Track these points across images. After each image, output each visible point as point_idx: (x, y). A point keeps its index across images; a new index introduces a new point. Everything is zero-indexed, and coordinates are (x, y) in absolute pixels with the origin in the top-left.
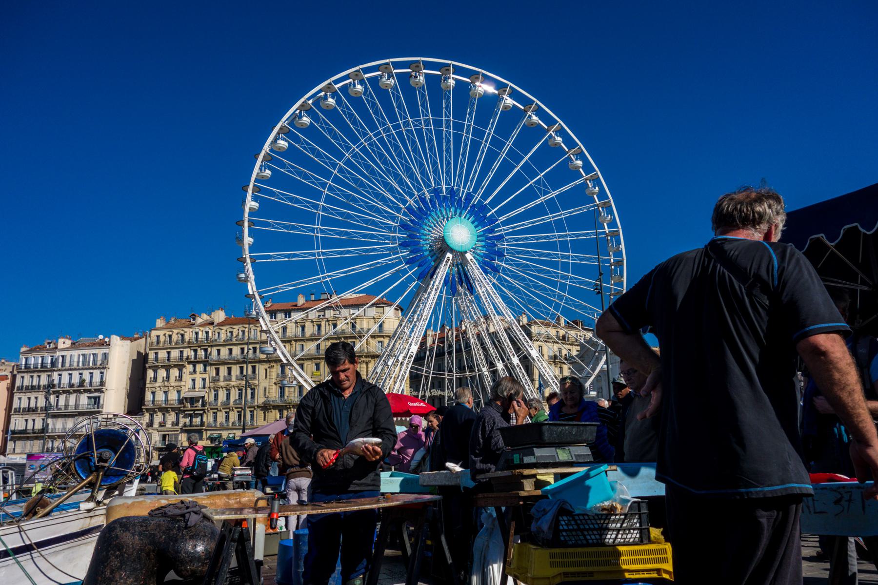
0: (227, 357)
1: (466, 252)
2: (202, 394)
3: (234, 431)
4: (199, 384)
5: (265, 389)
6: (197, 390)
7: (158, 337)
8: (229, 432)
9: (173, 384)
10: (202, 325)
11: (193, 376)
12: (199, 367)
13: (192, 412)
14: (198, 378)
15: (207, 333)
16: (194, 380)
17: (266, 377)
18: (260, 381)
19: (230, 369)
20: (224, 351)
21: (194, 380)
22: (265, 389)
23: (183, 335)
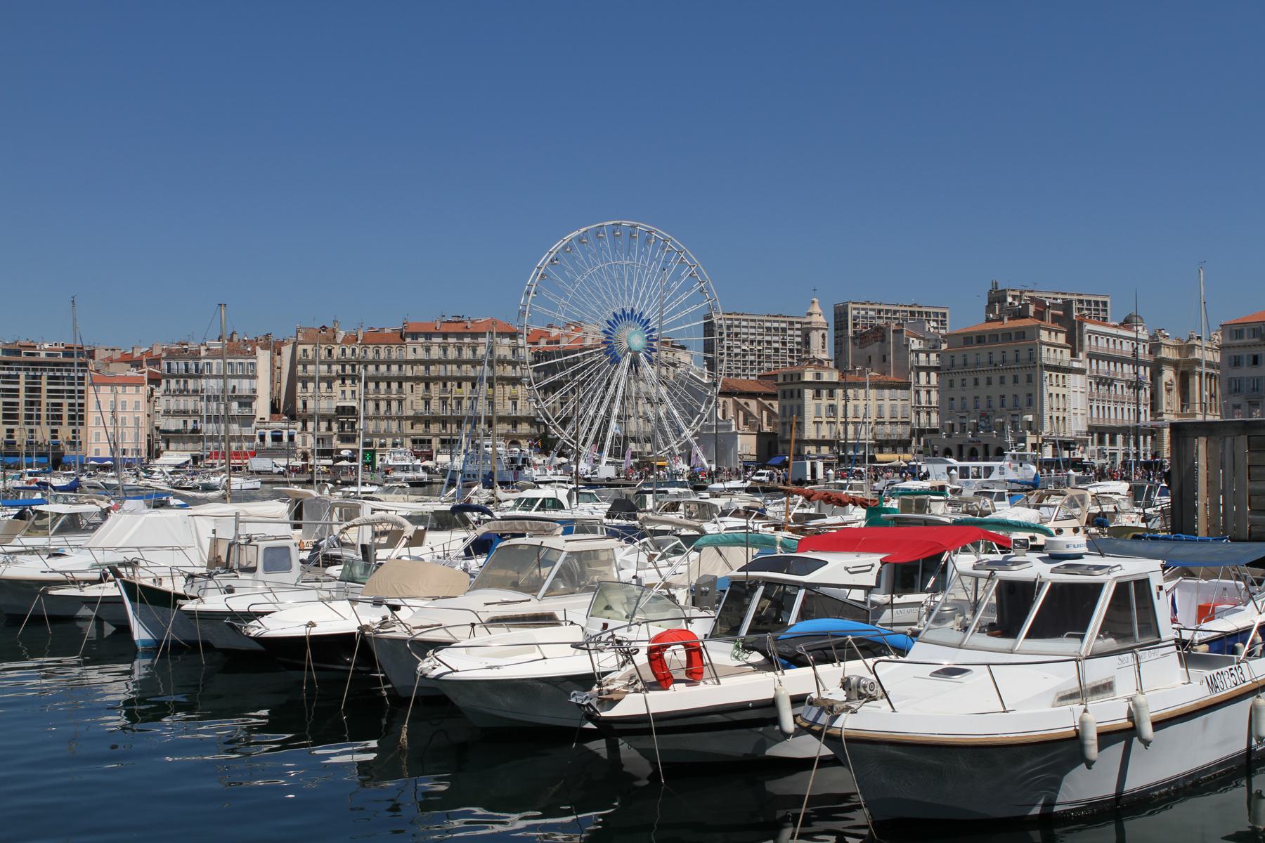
1: (640, 352)
2: (354, 404)
4: (348, 394)
5: (412, 402)
6: (348, 400)
7: (305, 351)
9: (324, 394)
10: (345, 341)
11: (343, 388)
15: (354, 350)
16: (343, 392)
17: (412, 392)
19: (389, 386)
21: (343, 392)
22: (412, 402)
23: (330, 351)
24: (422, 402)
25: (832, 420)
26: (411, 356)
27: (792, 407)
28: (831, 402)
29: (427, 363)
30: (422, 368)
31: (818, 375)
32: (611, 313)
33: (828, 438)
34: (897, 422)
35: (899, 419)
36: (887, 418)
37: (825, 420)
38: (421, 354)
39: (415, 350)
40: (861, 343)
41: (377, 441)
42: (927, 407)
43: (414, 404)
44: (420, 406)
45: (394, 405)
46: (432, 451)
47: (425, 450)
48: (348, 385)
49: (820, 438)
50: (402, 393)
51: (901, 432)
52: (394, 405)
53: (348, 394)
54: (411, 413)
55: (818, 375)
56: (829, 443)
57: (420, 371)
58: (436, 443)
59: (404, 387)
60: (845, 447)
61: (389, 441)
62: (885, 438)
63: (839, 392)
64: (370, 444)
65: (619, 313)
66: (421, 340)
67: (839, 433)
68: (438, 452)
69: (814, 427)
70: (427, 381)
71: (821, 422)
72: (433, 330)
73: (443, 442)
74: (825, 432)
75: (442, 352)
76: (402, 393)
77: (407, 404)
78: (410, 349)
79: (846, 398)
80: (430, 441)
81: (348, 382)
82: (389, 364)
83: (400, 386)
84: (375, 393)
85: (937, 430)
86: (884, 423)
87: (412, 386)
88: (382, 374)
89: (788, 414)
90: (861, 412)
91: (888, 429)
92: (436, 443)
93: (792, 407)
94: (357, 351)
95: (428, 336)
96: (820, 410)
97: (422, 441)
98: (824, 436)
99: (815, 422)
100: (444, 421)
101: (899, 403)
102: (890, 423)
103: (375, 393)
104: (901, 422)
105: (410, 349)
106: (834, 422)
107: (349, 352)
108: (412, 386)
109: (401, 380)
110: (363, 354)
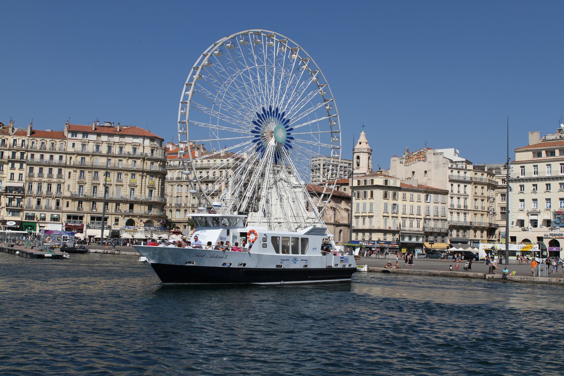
0: (39, 161)
2: (21, 185)
3: (45, 213)
4: (16, 177)
5: (69, 186)
8: (41, 213)
11: (12, 171)
12: (17, 165)
13: (13, 197)
14: (17, 173)
18: (65, 180)
20: (37, 156)
22: (69, 186)
24: (77, 186)
25: (395, 215)
26: (70, 149)
27: (365, 205)
28: (395, 202)
29: (83, 155)
30: (79, 158)
31: (386, 181)
32: (255, 113)
33: (392, 229)
34: (438, 220)
35: (440, 217)
36: (432, 217)
37: (390, 215)
38: (78, 147)
39: (74, 144)
40: (406, 162)
41: (37, 214)
42: (458, 210)
43: (71, 187)
44: (75, 189)
45: (54, 187)
46: (83, 226)
47: (77, 225)
48: (17, 169)
49: (387, 228)
50: (61, 178)
51: (441, 226)
52: (54, 187)
53: (16, 177)
54: (68, 194)
55: (386, 181)
56: (394, 232)
57: (77, 160)
58: (87, 219)
59: (63, 173)
60: (403, 236)
61: (48, 216)
62: (431, 231)
63: (400, 194)
64: (33, 217)
65: (267, 109)
66: (80, 136)
67: (400, 225)
68: (88, 227)
69: (382, 220)
70: (82, 168)
71: (388, 217)
72: (89, 131)
73: (93, 218)
74: (391, 224)
75: (95, 148)
76: (61, 178)
77: (64, 188)
78: (70, 143)
79: (404, 199)
80: (81, 218)
81: (17, 165)
82: (52, 152)
83: (60, 172)
84: (39, 176)
85: (523, 226)
86: (430, 219)
87: (70, 173)
88: (46, 162)
89: (361, 210)
90: (415, 211)
91: (432, 224)
92: (87, 219)
93: (365, 205)
94: (26, 143)
95: (85, 134)
96: (387, 207)
97: (75, 218)
98: (390, 227)
99: (384, 216)
100: (94, 201)
101: (440, 205)
102: (434, 219)
103: (39, 176)
104: (442, 220)
105: (70, 143)
106: (397, 217)
107: (19, 142)
108: (70, 173)
109: (61, 167)
110: (30, 144)
